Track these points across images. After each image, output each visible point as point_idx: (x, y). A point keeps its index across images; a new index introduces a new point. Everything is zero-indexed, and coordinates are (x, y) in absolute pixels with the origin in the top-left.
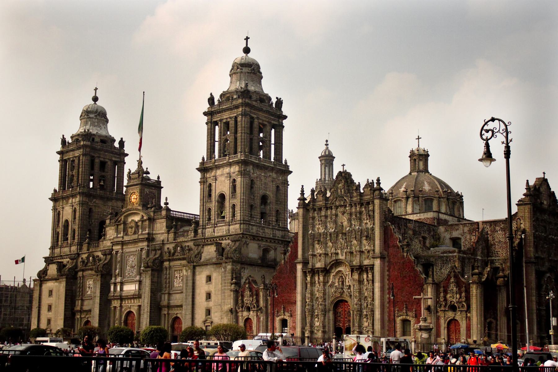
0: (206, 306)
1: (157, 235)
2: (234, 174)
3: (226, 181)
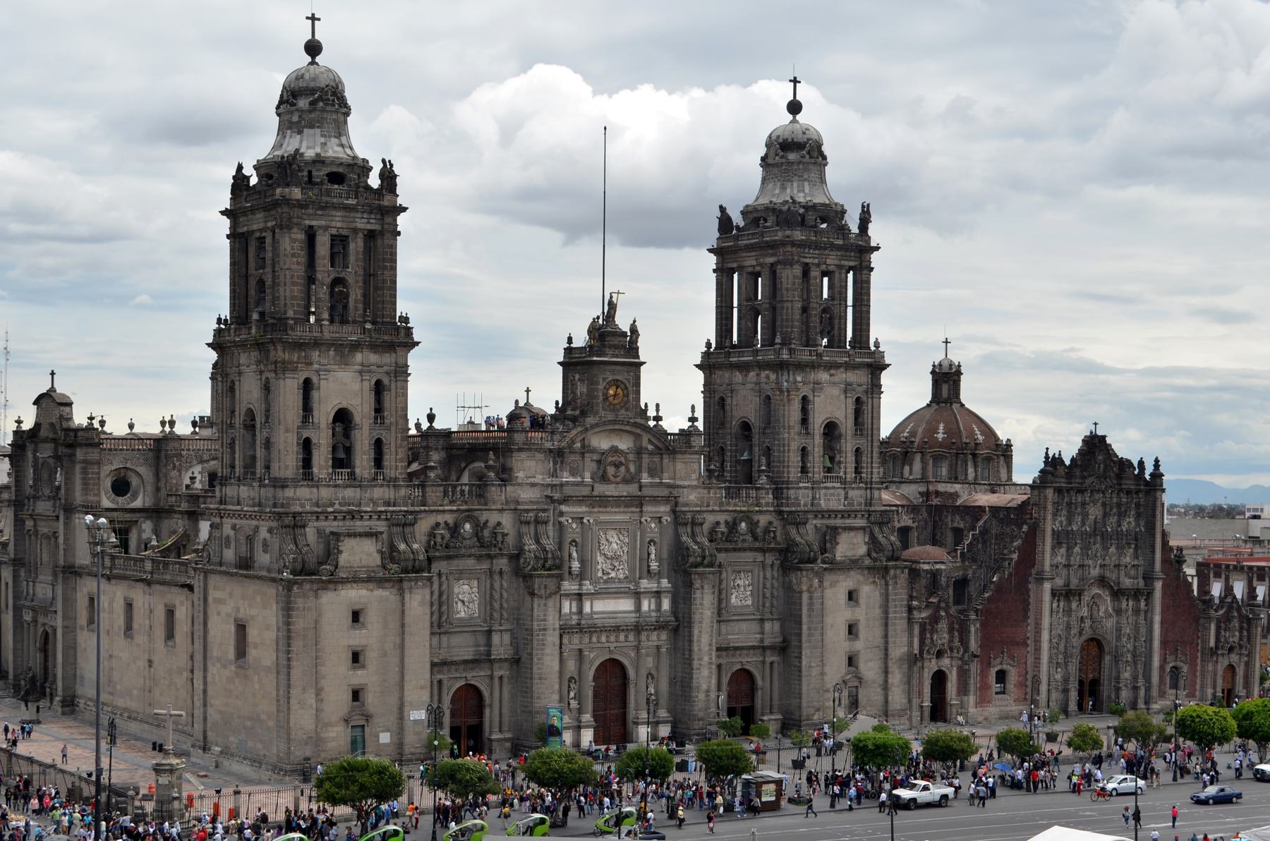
0: (848, 649)
1: (681, 490)
2: (861, 389)
3: (843, 397)
